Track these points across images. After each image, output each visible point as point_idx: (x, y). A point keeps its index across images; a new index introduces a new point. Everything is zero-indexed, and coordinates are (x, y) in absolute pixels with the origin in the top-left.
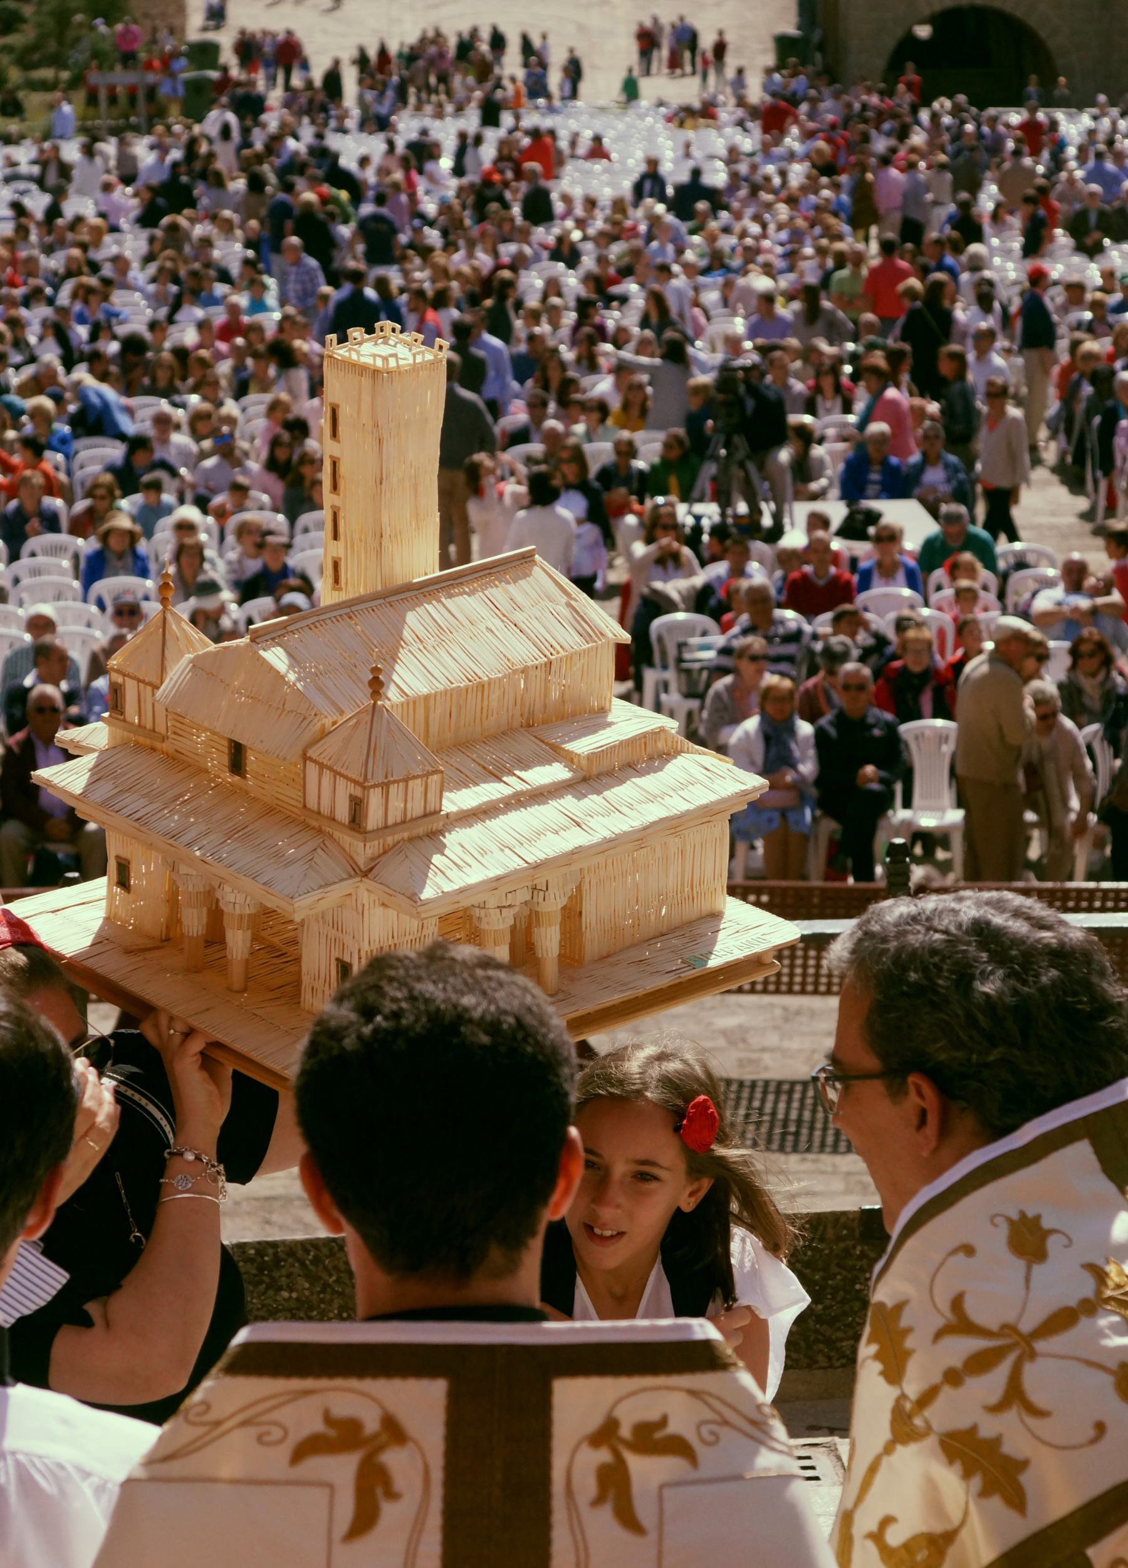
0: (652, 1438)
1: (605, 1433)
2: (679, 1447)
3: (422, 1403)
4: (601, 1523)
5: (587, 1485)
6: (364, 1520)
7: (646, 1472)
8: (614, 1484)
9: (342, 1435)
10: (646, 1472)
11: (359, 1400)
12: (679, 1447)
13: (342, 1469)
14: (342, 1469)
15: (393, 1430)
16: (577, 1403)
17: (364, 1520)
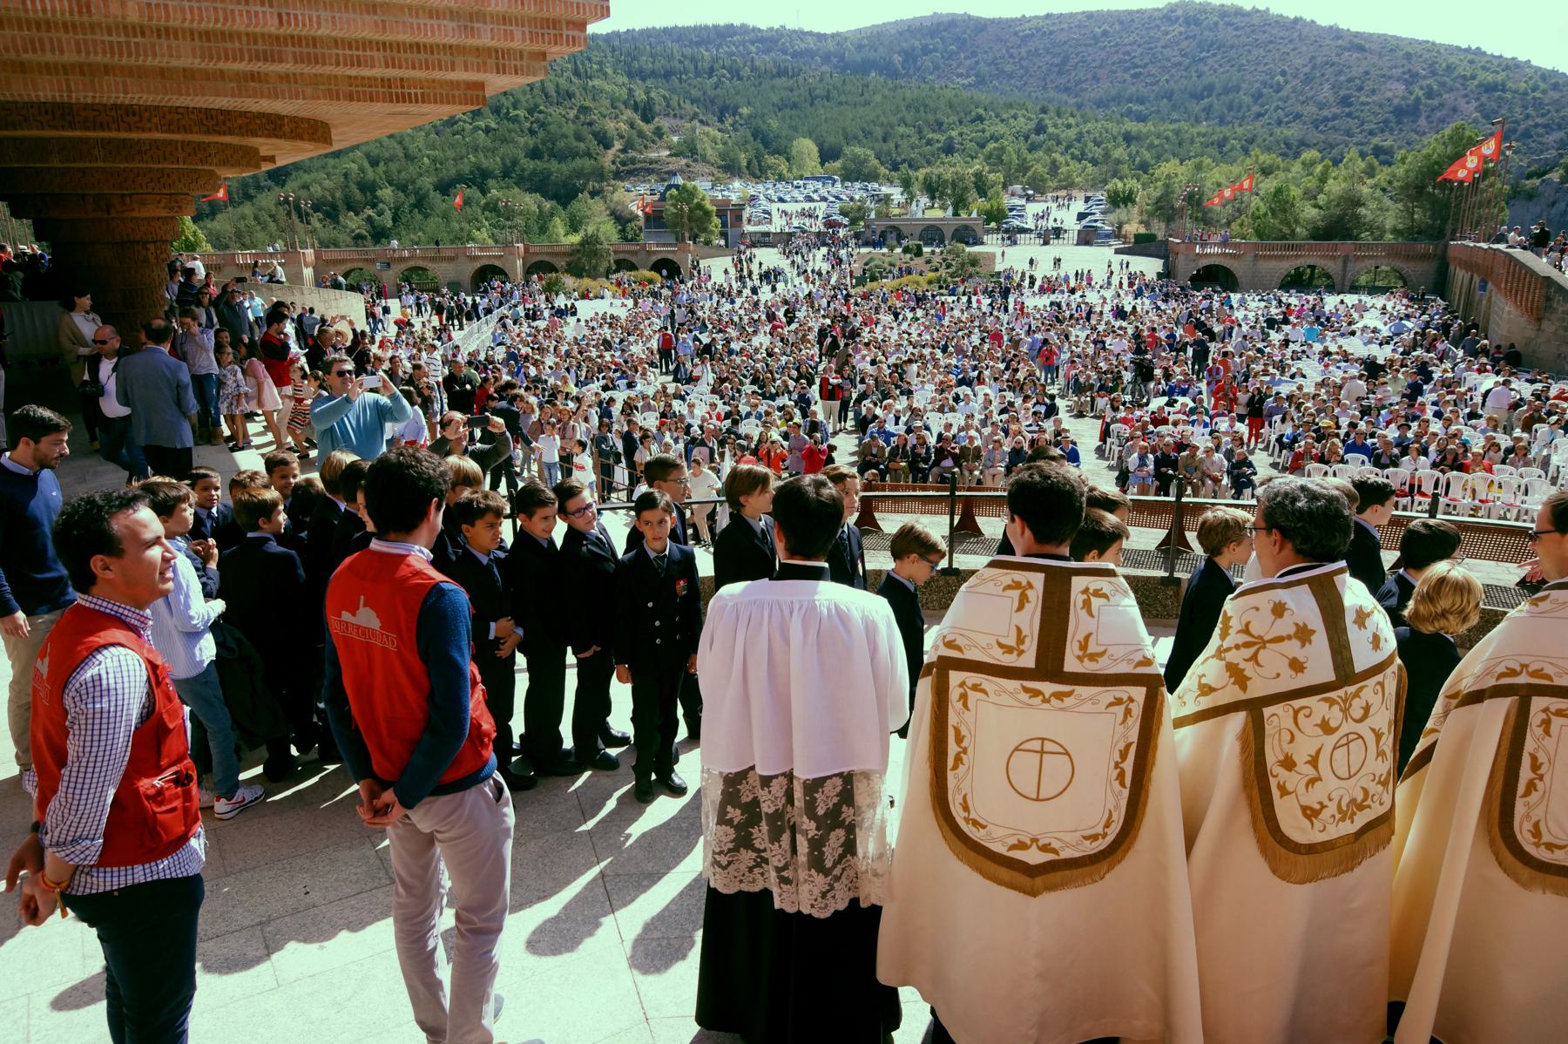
0: (1098, 593)
1: (1086, 591)
2: (1105, 596)
3: (1038, 579)
4: (1083, 613)
5: (1080, 604)
6: (1021, 608)
7: (1096, 602)
8: (1087, 604)
9: (1016, 585)
10: (1096, 602)
11: (1022, 577)
12: (1105, 596)
13: (1016, 593)
14: (1016, 593)
15: (1030, 585)
16: (1078, 583)
17: (1021, 608)
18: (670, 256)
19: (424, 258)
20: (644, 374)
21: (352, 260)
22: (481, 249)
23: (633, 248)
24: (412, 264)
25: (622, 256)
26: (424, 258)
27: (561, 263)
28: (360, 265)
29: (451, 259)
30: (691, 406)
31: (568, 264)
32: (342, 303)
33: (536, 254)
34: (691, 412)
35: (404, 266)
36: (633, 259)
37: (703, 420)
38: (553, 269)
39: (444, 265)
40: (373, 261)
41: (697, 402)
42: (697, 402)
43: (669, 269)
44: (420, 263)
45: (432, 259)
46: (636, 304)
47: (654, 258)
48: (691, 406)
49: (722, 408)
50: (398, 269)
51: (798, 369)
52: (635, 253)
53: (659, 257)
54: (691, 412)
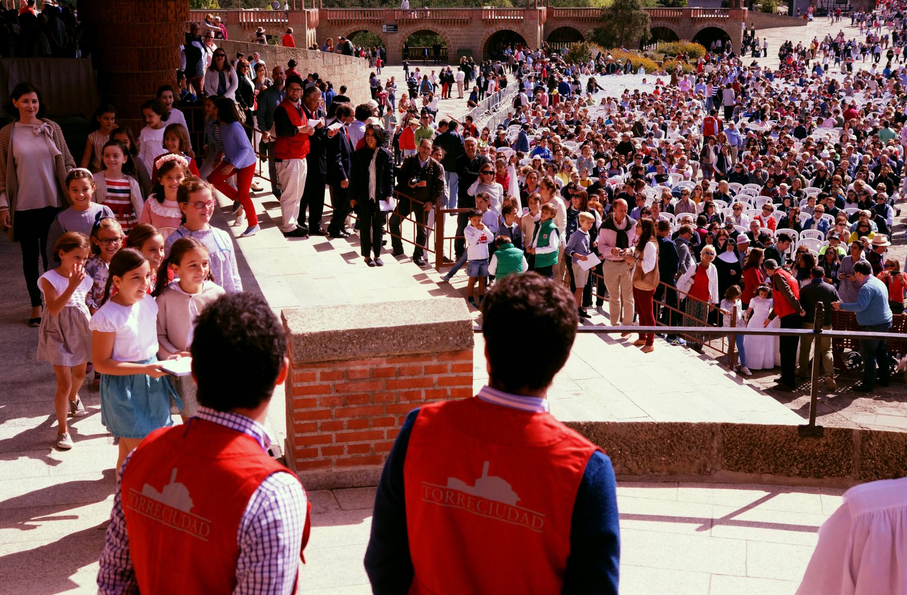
18: (719, 25)
19: (434, 21)
20: (681, 166)
21: (358, 22)
22: (499, 12)
23: (676, 14)
24: (421, 27)
25: (660, 24)
26: (434, 21)
27: (588, 30)
28: (365, 27)
29: (463, 23)
30: (737, 209)
31: (597, 32)
32: (346, 69)
33: (559, 19)
34: (737, 216)
35: (412, 29)
36: (674, 27)
37: (753, 225)
38: (576, 36)
39: (456, 29)
40: (379, 23)
41: (745, 204)
42: (745, 204)
43: (712, 38)
44: (430, 27)
45: (444, 23)
46: (674, 82)
47: (699, 27)
48: (737, 209)
49: (778, 215)
50: (405, 33)
51: (876, 170)
52: (675, 20)
53: (706, 25)
54: (737, 216)
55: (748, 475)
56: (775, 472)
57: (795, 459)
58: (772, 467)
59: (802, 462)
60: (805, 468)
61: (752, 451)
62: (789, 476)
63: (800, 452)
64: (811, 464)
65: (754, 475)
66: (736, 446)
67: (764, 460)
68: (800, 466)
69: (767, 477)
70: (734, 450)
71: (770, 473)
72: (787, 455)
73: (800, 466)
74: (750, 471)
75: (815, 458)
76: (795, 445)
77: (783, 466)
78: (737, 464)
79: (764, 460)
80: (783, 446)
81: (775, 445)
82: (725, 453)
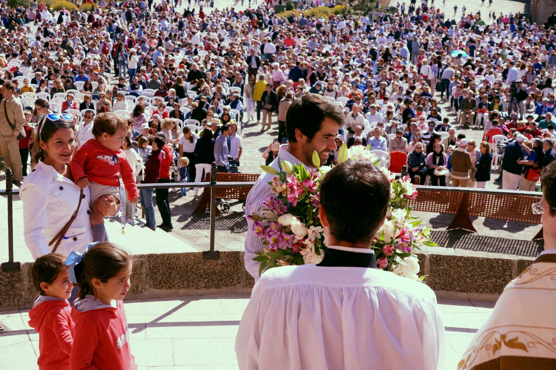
55: (169, 290)
56: (187, 287)
57: (202, 276)
58: (186, 283)
59: (206, 278)
60: (208, 282)
61: (171, 273)
62: (197, 288)
63: (205, 271)
64: (212, 279)
65: (173, 291)
66: (159, 270)
67: (180, 278)
68: (206, 280)
69: (182, 291)
70: (158, 273)
71: (184, 288)
72: (196, 274)
73: (206, 280)
74: (170, 288)
75: (215, 274)
76: (200, 266)
77: (193, 282)
78: (160, 284)
79: (180, 278)
80: (193, 268)
81: (187, 267)
82: (152, 276)
